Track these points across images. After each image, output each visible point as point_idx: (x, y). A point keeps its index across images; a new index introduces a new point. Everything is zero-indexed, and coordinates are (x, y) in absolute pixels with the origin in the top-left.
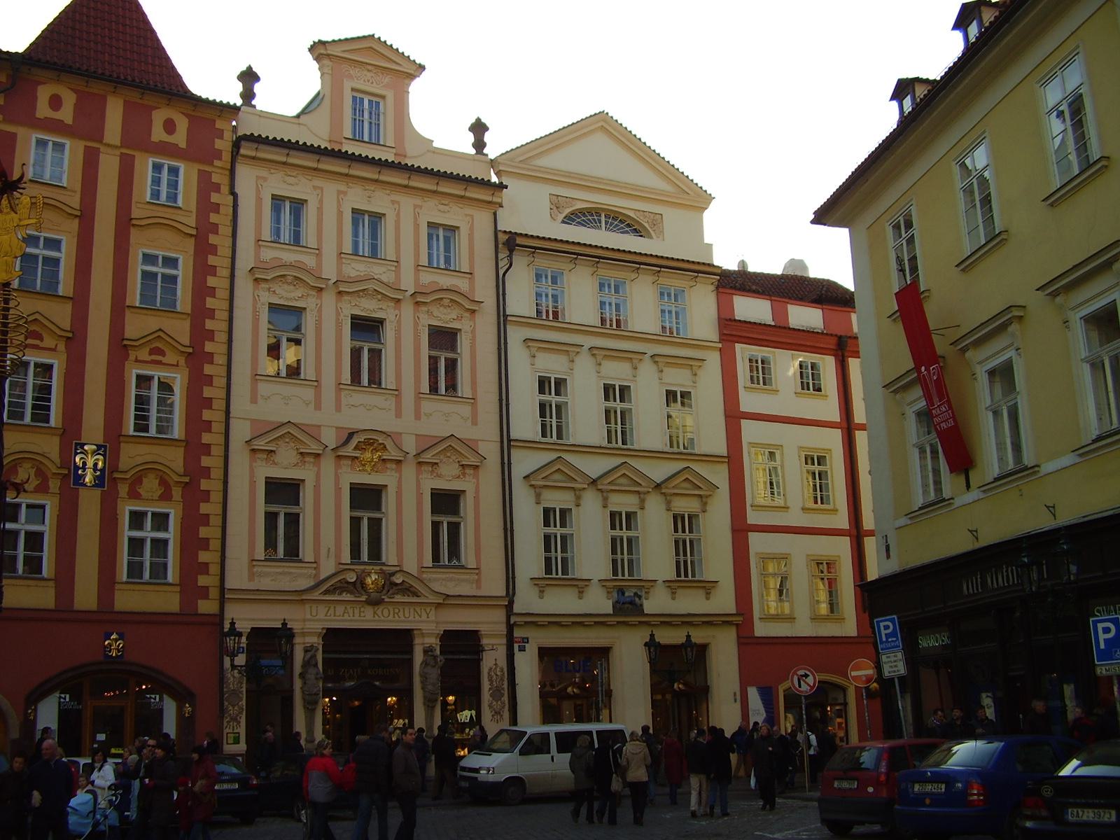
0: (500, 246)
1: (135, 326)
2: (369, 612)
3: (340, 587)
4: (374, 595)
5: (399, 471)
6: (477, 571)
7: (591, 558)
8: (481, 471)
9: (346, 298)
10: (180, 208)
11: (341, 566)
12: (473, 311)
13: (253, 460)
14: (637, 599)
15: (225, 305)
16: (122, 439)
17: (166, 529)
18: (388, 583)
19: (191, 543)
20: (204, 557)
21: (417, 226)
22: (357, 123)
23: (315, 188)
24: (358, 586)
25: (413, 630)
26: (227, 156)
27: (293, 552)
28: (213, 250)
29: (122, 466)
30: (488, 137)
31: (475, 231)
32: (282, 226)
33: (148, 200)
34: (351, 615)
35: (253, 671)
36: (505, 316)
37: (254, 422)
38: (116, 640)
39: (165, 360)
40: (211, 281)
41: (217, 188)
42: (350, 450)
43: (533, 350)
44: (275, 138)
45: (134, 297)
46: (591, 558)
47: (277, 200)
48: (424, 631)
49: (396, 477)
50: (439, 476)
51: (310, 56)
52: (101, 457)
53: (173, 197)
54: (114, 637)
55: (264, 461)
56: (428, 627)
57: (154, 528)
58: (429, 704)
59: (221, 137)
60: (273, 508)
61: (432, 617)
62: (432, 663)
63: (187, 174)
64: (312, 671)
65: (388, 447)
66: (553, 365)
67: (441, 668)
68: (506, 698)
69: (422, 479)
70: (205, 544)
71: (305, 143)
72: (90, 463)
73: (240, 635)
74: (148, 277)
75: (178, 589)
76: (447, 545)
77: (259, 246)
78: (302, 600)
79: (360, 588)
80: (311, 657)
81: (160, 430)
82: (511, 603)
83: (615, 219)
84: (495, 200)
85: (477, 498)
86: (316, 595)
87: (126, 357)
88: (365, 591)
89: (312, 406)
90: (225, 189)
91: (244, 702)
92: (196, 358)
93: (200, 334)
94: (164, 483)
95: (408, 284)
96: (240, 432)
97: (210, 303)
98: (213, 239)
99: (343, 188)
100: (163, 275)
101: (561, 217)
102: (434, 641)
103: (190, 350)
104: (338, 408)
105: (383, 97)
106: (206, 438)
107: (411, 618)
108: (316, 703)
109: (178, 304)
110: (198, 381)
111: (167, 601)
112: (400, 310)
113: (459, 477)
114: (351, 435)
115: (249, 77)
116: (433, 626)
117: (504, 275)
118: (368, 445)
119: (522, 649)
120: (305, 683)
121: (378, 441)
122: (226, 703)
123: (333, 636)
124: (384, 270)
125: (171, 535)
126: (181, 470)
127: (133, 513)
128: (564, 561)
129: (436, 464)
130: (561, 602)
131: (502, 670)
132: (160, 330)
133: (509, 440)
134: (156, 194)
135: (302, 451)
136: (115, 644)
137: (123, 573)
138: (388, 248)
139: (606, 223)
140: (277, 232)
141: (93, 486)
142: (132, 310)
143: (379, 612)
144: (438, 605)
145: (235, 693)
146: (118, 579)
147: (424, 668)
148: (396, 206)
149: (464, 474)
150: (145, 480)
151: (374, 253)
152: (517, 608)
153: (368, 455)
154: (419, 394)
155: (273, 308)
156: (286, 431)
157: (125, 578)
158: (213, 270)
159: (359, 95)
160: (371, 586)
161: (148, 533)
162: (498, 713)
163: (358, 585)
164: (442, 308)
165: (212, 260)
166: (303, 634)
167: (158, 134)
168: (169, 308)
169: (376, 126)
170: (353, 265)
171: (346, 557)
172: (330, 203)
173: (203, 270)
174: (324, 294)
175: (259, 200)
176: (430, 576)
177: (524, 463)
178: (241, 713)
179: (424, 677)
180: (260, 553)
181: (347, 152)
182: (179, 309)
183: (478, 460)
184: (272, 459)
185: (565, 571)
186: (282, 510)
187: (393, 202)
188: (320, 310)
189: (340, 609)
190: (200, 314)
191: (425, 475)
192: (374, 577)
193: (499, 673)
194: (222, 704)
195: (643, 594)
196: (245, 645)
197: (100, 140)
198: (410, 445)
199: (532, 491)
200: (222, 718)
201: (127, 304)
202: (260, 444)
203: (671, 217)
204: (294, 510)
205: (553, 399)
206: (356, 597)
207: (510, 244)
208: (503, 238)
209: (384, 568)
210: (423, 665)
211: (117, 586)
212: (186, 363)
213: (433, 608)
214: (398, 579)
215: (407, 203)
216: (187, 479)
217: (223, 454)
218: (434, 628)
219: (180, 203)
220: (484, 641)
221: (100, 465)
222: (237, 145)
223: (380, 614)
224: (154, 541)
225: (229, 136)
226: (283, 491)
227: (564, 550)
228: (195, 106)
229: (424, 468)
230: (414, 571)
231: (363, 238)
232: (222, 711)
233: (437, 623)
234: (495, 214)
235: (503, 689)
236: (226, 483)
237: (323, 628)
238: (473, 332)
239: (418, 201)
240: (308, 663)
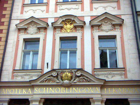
3: (50, 79)
6: (124, 69)
25: (89, 98)
42: (58, 24)
48: (94, 99)
49: (81, 33)
55: (24, 33)
65: (76, 21)
69: (93, 32)
79: (60, 79)
88: (62, 80)
96: (14, 23)
104: (56, 11)
113: (112, 30)
118: (68, 22)
121: (71, 19)
153: (68, 26)
156: (32, 21)
176: (98, 73)
183: (121, 21)
184: (27, 32)
191: (95, 31)
198: (87, 20)
213: (100, 88)
218: (100, 97)
230: (90, 72)
233: (102, 95)
236: (6, 41)
237: (41, 98)
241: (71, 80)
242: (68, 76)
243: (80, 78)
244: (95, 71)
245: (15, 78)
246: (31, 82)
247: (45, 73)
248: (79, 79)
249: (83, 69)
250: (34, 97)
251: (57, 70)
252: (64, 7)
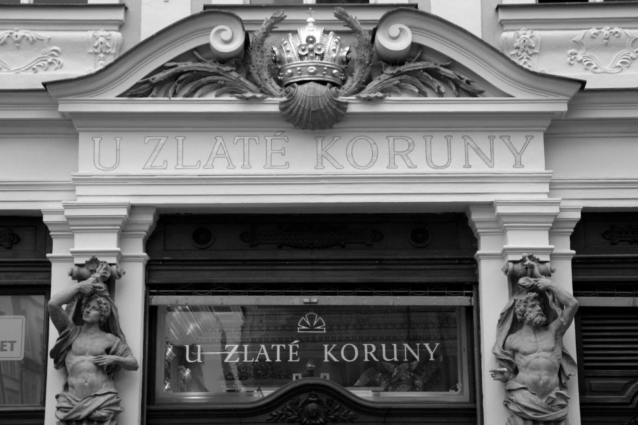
25: (467, 206)
48: (500, 210)
62: (534, 313)
79: (266, 75)
88: (280, 83)
120: (66, 387)
147: (511, 332)
160: (297, 62)
176: (525, 34)
179: (510, 366)
206: (248, 100)
210: (507, 326)
214: (396, 39)
218: (544, 198)
237: (133, 209)
241: (344, 82)
242: (322, 57)
244: (502, 24)
246: (52, 91)
247: (148, 30)
248: (394, 76)
249: (421, 8)
250: (80, 201)
251: (245, 16)
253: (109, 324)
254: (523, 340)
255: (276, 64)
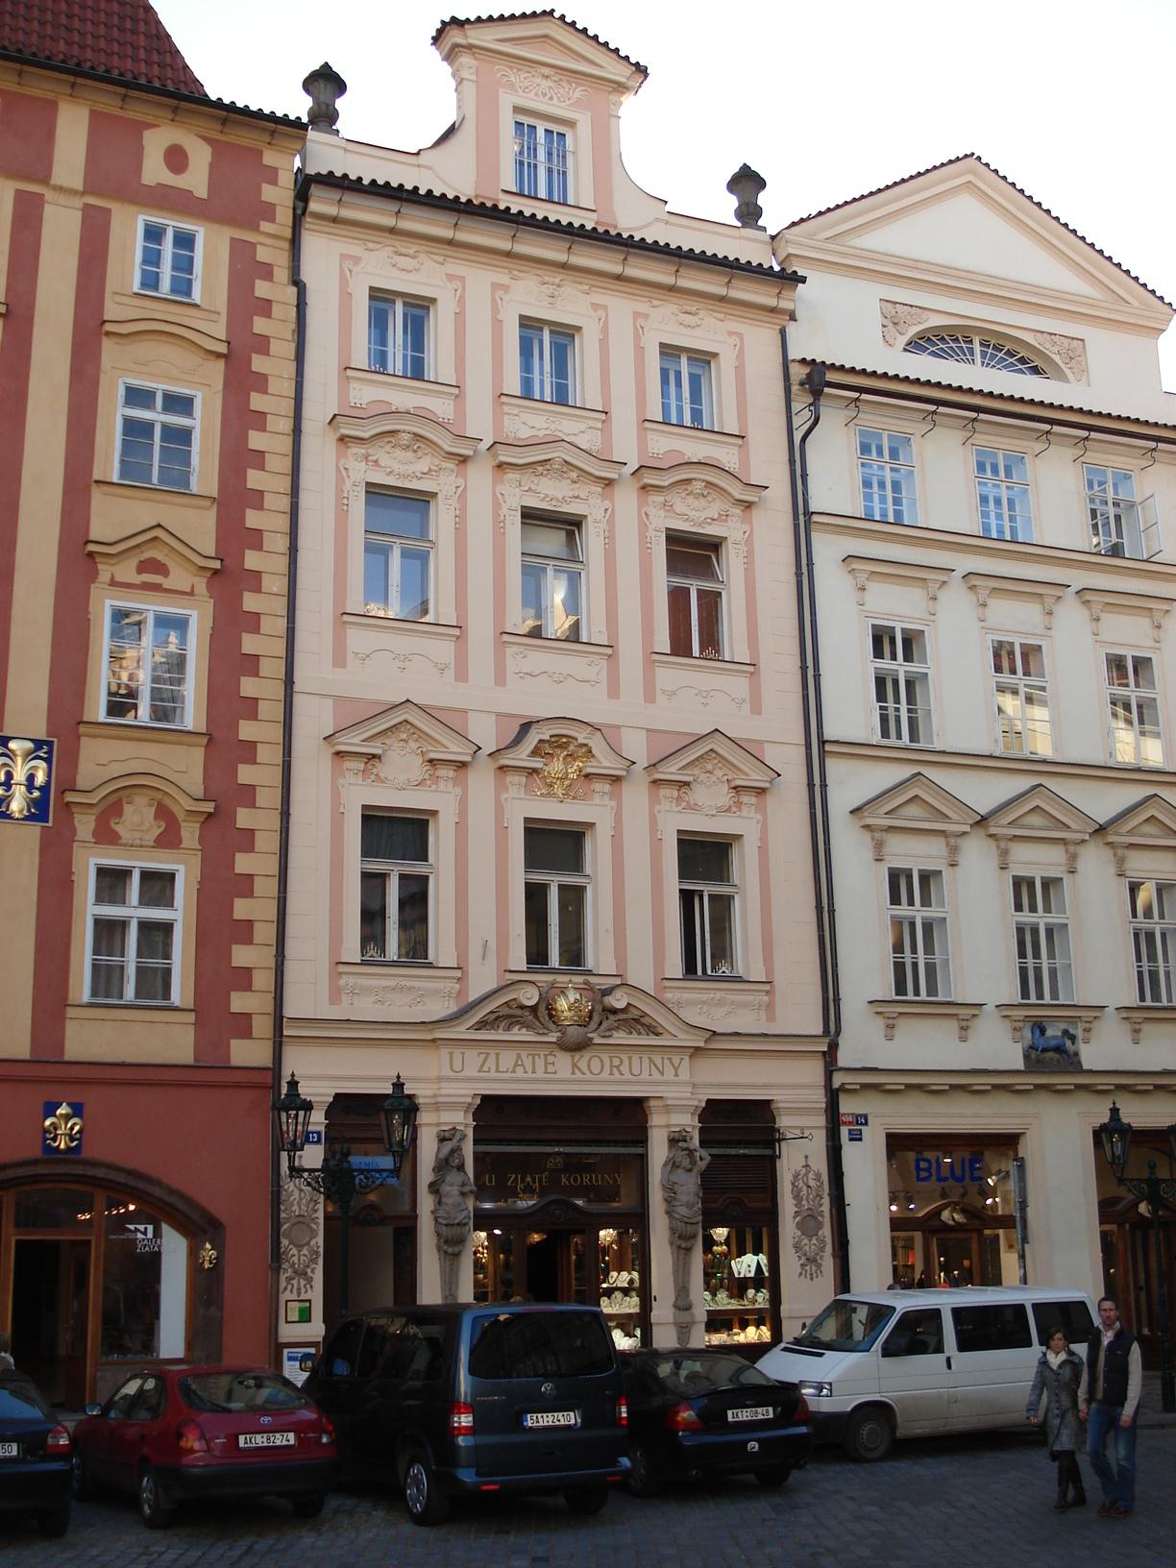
0: (795, 388)
1: (112, 518)
2: (563, 1062)
3: (509, 1016)
4: (574, 1033)
5: (617, 796)
7: (981, 961)
8: (770, 800)
9: (512, 476)
10: (196, 306)
11: (509, 976)
12: (748, 505)
13: (337, 773)
14: (1068, 1043)
15: (285, 484)
16: (82, 729)
17: (169, 903)
18: (599, 1007)
19: (219, 930)
20: (241, 956)
21: (640, 351)
22: (524, 167)
23: (450, 277)
24: (543, 1013)
26: (284, 216)
27: (416, 950)
28: (261, 383)
29: (82, 782)
30: (763, 199)
31: (747, 361)
32: (390, 349)
33: (136, 289)
34: (529, 1069)
35: (336, 1180)
36: (808, 514)
37: (339, 700)
38: (67, 1118)
39: (167, 583)
40: (256, 440)
41: (267, 272)
43: (862, 578)
44: (373, 182)
45: (109, 460)
46: (981, 961)
47: (380, 298)
50: (693, 808)
51: (434, 55)
52: (43, 765)
53: (183, 287)
54: (63, 1110)
56: (675, 1095)
57: (145, 901)
58: (681, 1243)
59: (274, 182)
60: (377, 866)
61: (684, 1074)
62: (686, 1163)
63: (211, 245)
64: (453, 1177)
66: (898, 606)
67: (703, 1174)
68: (826, 1232)
70: (245, 932)
71: (430, 192)
72: (20, 775)
73: (308, 1106)
74: (132, 427)
75: (191, 1017)
76: (705, 937)
77: (348, 378)
78: (434, 1040)
80: (452, 1152)
81: (160, 713)
82: (834, 1047)
83: (998, 348)
84: (784, 304)
85: (763, 850)
86: (461, 1031)
87: (93, 575)
89: (450, 674)
90: (282, 274)
91: (320, 1240)
92: (227, 578)
93: (236, 537)
94: (163, 813)
95: (627, 449)
96: (313, 719)
97: (254, 479)
98: (258, 363)
99: (503, 278)
100: (165, 427)
101: (903, 340)
102: (688, 1122)
103: (217, 565)
104: (500, 679)
105: (571, 124)
106: (247, 730)
107: (645, 1076)
108: (461, 1241)
109: (194, 480)
110: (231, 623)
111: (168, 1040)
112: (612, 501)
114: (526, 727)
115: (325, 82)
116: (685, 1092)
117: (804, 439)
119: (856, 1137)
122: (285, 1242)
123: (493, 1112)
124: (583, 427)
125: (180, 913)
126: (198, 790)
127: (102, 872)
128: (931, 969)
129: (687, 784)
130: (926, 1046)
131: (818, 1177)
132: (159, 525)
133: (822, 742)
134: (151, 281)
135: (432, 756)
136: (64, 1127)
137: (82, 986)
138: (586, 386)
139: (984, 355)
140: (380, 359)
141: (26, 818)
142: (106, 488)
143: (583, 1064)
144: (697, 1051)
145: (302, 1221)
146: (72, 998)
148: (601, 313)
149: (739, 804)
150: (128, 809)
151: (561, 398)
152: (844, 1059)
153: (557, 766)
154: (651, 655)
155: (375, 493)
157: (86, 996)
158: (259, 420)
159: (527, 120)
161: (133, 910)
162: (811, 1261)
163: (542, 1012)
164: (690, 499)
165: (257, 401)
166: (437, 1107)
167: (154, 171)
168: (176, 483)
169: (559, 176)
170: (524, 417)
171: (518, 958)
172: (479, 306)
173: (240, 419)
174: (471, 469)
175: (346, 297)
177: (852, 784)
178: (314, 1261)
179: (670, 1189)
180: (352, 946)
181: (508, 209)
182: (194, 488)
185: (932, 990)
186: (395, 870)
187: (595, 306)
188: (462, 498)
189: (508, 1058)
190: (234, 500)
192: (573, 996)
193: (812, 1183)
194: (276, 1244)
195: (1079, 1033)
196: (322, 1129)
197: (45, 179)
198: (636, 747)
199: (867, 836)
200: (277, 1270)
201: (96, 476)
202: (353, 742)
203: (1103, 347)
204: (416, 868)
205: (901, 668)
207: (817, 382)
208: (798, 372)
209: (592, 980)
211: (71, 1012)
212: (209, 587)
214: (618, 1000)
215: (621, 308)
216: (210, 807)
217: (280, 761)
219: (197, 296)
220: (783, 1122)
221: (40, 778)
222: (302, 195)
223: (585, 1069)
224: (145, 926)
225: (287, 180)
226: (396, 833)
227: (929, 949)
228: (224, 122)
229: (665, 792)
231: (542, 373)
232: (277, 1256)
233: (694, 1086)
234: (783, 333)
235: (821, 1213)
236: (285, 814)
238: (749, 542)
239: (642, 306)
240: (443, 1166)
243: (622, 1016)
245: (345, 999)
252: (538, 659)
253: (461, 1168)
254: (680, 1176)
255: (552, 1013)
